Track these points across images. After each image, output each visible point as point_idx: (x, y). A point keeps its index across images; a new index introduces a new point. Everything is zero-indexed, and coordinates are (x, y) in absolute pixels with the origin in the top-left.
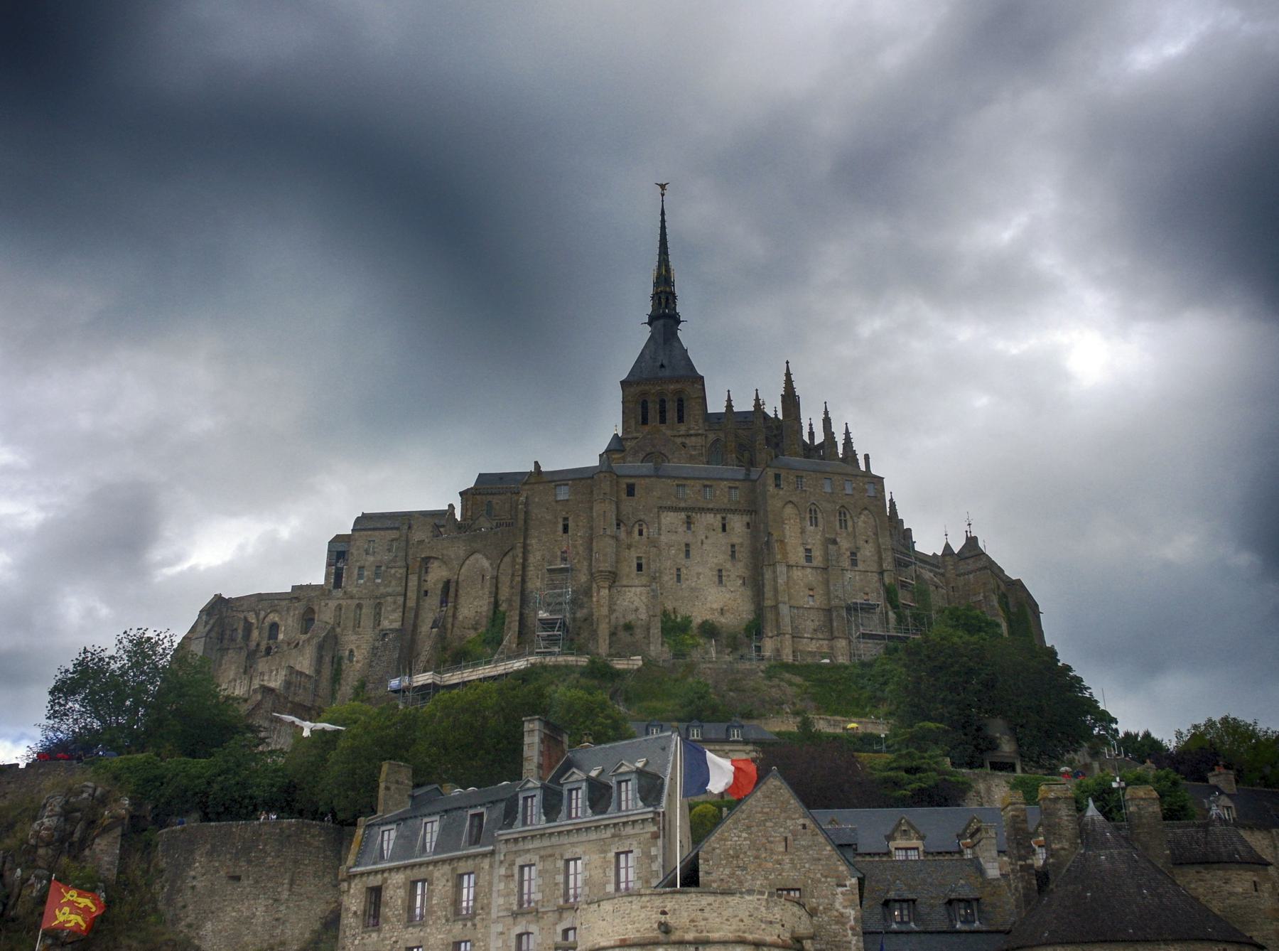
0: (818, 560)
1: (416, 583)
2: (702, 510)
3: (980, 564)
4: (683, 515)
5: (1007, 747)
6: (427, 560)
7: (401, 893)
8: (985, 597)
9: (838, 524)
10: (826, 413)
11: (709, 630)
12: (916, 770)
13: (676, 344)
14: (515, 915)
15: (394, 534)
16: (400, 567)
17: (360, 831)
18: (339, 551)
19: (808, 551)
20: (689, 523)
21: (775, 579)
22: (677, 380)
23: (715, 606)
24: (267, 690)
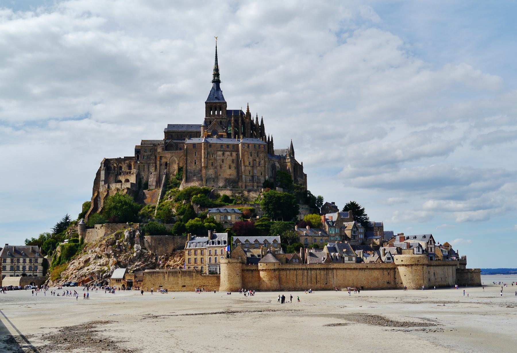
0: (251, 165)
4: (222, 152)
9: (256, 156)
10: (257, 116)
14: (209, 255)
16: (154, 156)
17: (186, 243)
18: (138, 151)
19: (249, 162)
20: (223, 154)
22: (220, 103)
23: (229, 174)
24: (128, 189)
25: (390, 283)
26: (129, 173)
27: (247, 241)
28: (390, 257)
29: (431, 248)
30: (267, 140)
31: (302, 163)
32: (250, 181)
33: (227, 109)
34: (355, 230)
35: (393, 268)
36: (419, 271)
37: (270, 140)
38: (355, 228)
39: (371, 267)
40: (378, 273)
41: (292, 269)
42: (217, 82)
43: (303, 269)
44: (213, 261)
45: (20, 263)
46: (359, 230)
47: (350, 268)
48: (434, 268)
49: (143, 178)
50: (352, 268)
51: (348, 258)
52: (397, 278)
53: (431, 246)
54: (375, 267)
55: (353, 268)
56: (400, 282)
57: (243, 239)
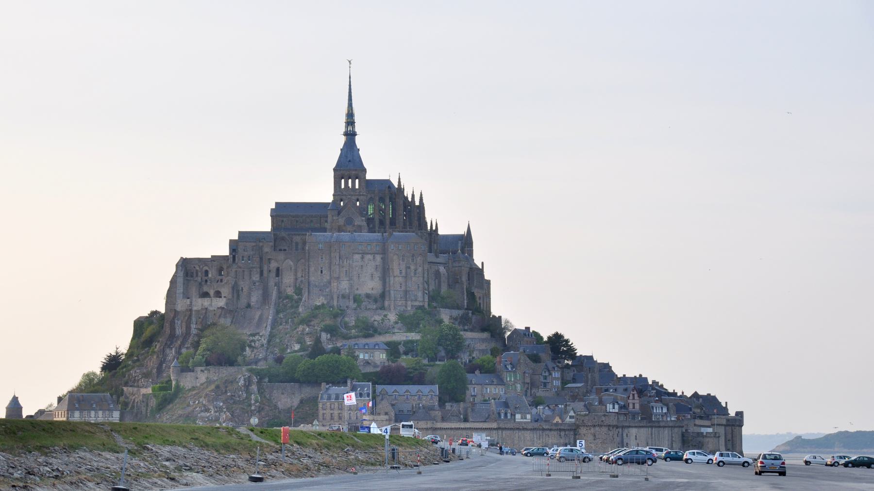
0: (404, 274)
1: (267, 268)
2: (368, 254)
3: (460, 265)
4: (360, 255)
5: (443, 353)
6: (269, 259)
7: (329, 405)
8: (460, 277)
10: (413, 192)
11: (368, 296)
12: (416, 370)
13: (355, 148)
14: (349, 410)
15: (254, 244)
16: (258, 257)
20: (362, 258)
21: (390, 281)
24: (222, 308)
26: (219, 281)
27: (395, 391)
29: (634, 404)
30: (429, 228)
31: (483, 263)
32: (401, 298)
33: (369, 177)
34: (547, 374)
37: (434, 228)
41: (449, 428)
42: (350, 135)
43: (462, 428)
44: (354, 418)
45: (91, 417)
46: (553, 374)
49: (242, 289)
53: (633, 401)
57: (390, 389)
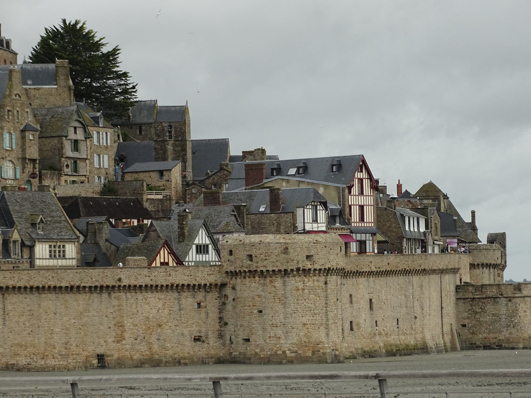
25: (203, 342)
28: (208, 242)
29: (362, 208)
34: (80, 135)
35: (216, 285)
36: (312, 296)
38: (80, 132)
39: (133, 282)
40: (160, 305)
47: (55, 287)
48: (372, 284)
50: (61, 287)
51: (50, 246)
52: (231, 322)
53: (361, 200)
54: (150, 283)
55: (67, 287)
56: (243, 335)
